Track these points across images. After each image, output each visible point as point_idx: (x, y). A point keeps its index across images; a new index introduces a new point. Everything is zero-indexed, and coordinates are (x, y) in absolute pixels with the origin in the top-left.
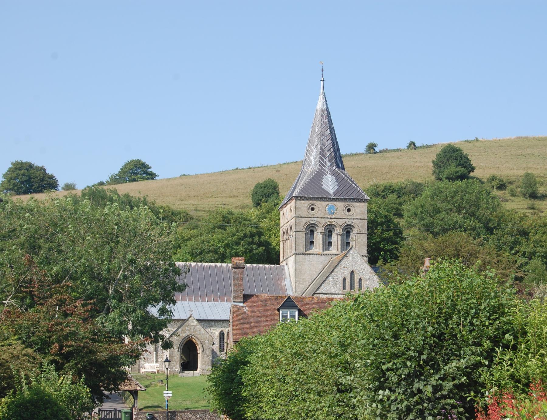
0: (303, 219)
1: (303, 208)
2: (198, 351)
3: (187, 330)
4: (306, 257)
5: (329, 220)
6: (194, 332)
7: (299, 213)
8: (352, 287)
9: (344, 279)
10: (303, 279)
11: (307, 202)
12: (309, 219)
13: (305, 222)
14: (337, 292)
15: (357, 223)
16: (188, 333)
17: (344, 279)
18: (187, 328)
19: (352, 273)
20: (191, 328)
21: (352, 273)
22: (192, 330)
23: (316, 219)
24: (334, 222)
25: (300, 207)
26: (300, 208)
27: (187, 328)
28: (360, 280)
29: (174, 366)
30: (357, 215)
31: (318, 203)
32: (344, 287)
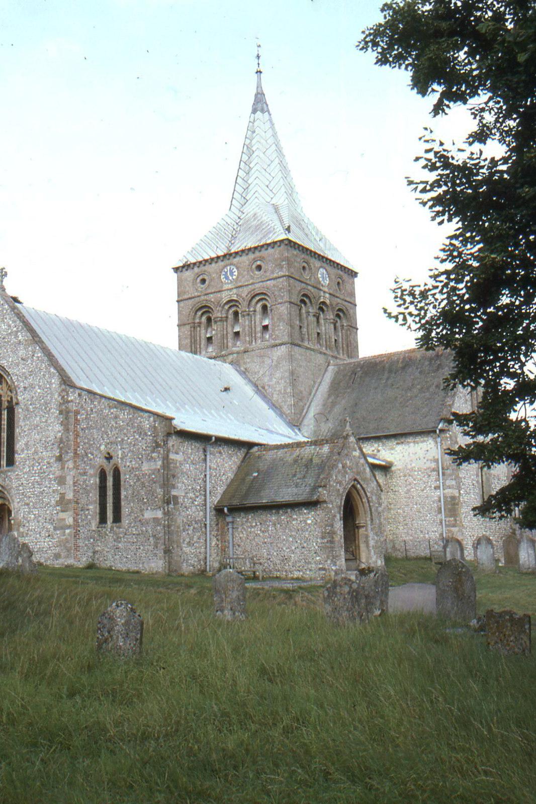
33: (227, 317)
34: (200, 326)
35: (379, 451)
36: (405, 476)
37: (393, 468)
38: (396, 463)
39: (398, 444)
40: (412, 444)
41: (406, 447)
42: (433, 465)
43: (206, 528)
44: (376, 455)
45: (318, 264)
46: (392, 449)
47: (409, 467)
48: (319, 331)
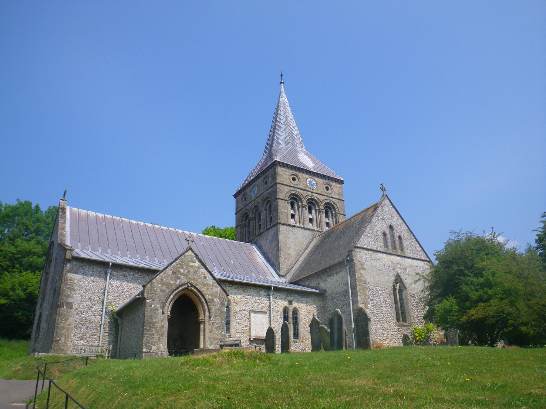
0: (286, 187)
1: (284, 176)
2: (201, 317)
3: (183, 274)
4: (290, 228)
5: (310, 193)
6: (194, 279)
7: (281, 179)
8: (394, 247)
9: (384, 234)
10: (289, 254)
11: (287, 170)
12: (292, 189)
13: (287, 190)
14: (379, 249)
15: (336, 202)
16: (184, 280)
17: (384, 234)
18: (182, 271)
19: (391, 227)
20: (189, 272)
21: (391, 227)
22: (191, 276)
23: (297, 190)
24: (315, 196)
25: (282, 173)
26: (282, 175)
27: (182, 271)
28: (400, 237)
29: (154, 343)
30: (335, 195)
31: (300, 174)
32: (386, 245)
33: (255, 217)
34: (245, 226)
35: (319, 283)
36: (332, 299)
37: (327, 294)
38: (328, 290)
39: (328, 276)
40: (335, 275)
41: (332, 278)
42: (345, 288)
43: (101, 327)
44: (318, 287)
45: (306, 176)
46: (325, 281)
47: (334, 292)
48: (311, 217)
